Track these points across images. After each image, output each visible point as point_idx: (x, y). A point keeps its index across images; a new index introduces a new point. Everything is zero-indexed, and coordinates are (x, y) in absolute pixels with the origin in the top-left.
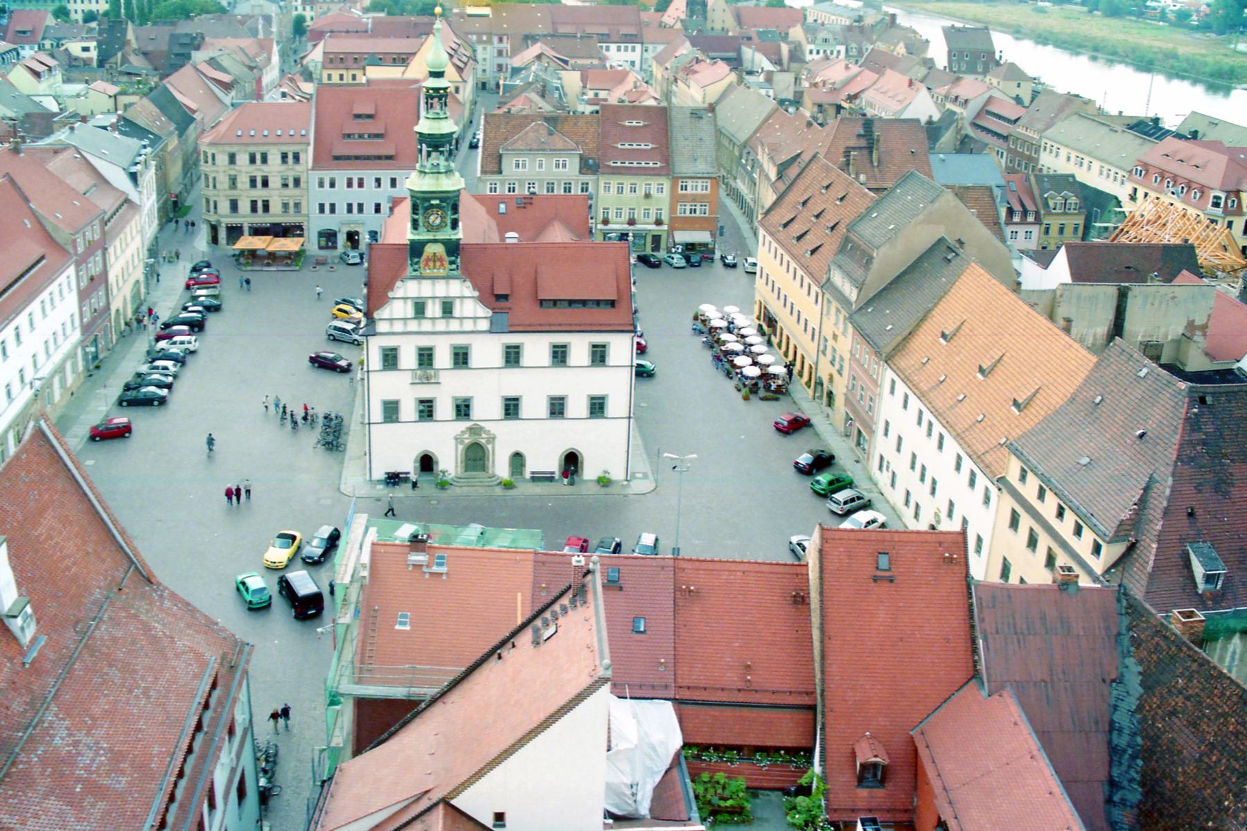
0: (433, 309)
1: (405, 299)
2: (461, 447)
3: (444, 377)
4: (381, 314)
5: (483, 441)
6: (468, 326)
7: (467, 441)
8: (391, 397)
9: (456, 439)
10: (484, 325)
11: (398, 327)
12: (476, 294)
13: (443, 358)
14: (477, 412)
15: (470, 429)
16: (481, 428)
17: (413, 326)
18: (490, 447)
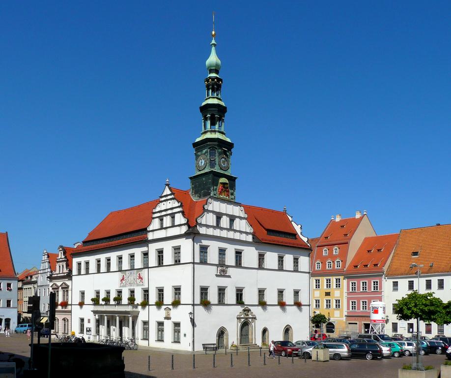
0: (225, 222)
1: (213, 212)
2: (239, 324)
3: (230, 271)
4: (203, 220)
5: (250, 320)
6: (243, 237)
7: (242, 320)
8: (205, 284)
9: (238, 318)
10: (250, 238)
11: (210, 232)
12: (246, 216)
13: (230, 259)
14: (246, 299)
15: (244, 310)
16: (249, 310)
17: (217, 233)
18: (253, 324)
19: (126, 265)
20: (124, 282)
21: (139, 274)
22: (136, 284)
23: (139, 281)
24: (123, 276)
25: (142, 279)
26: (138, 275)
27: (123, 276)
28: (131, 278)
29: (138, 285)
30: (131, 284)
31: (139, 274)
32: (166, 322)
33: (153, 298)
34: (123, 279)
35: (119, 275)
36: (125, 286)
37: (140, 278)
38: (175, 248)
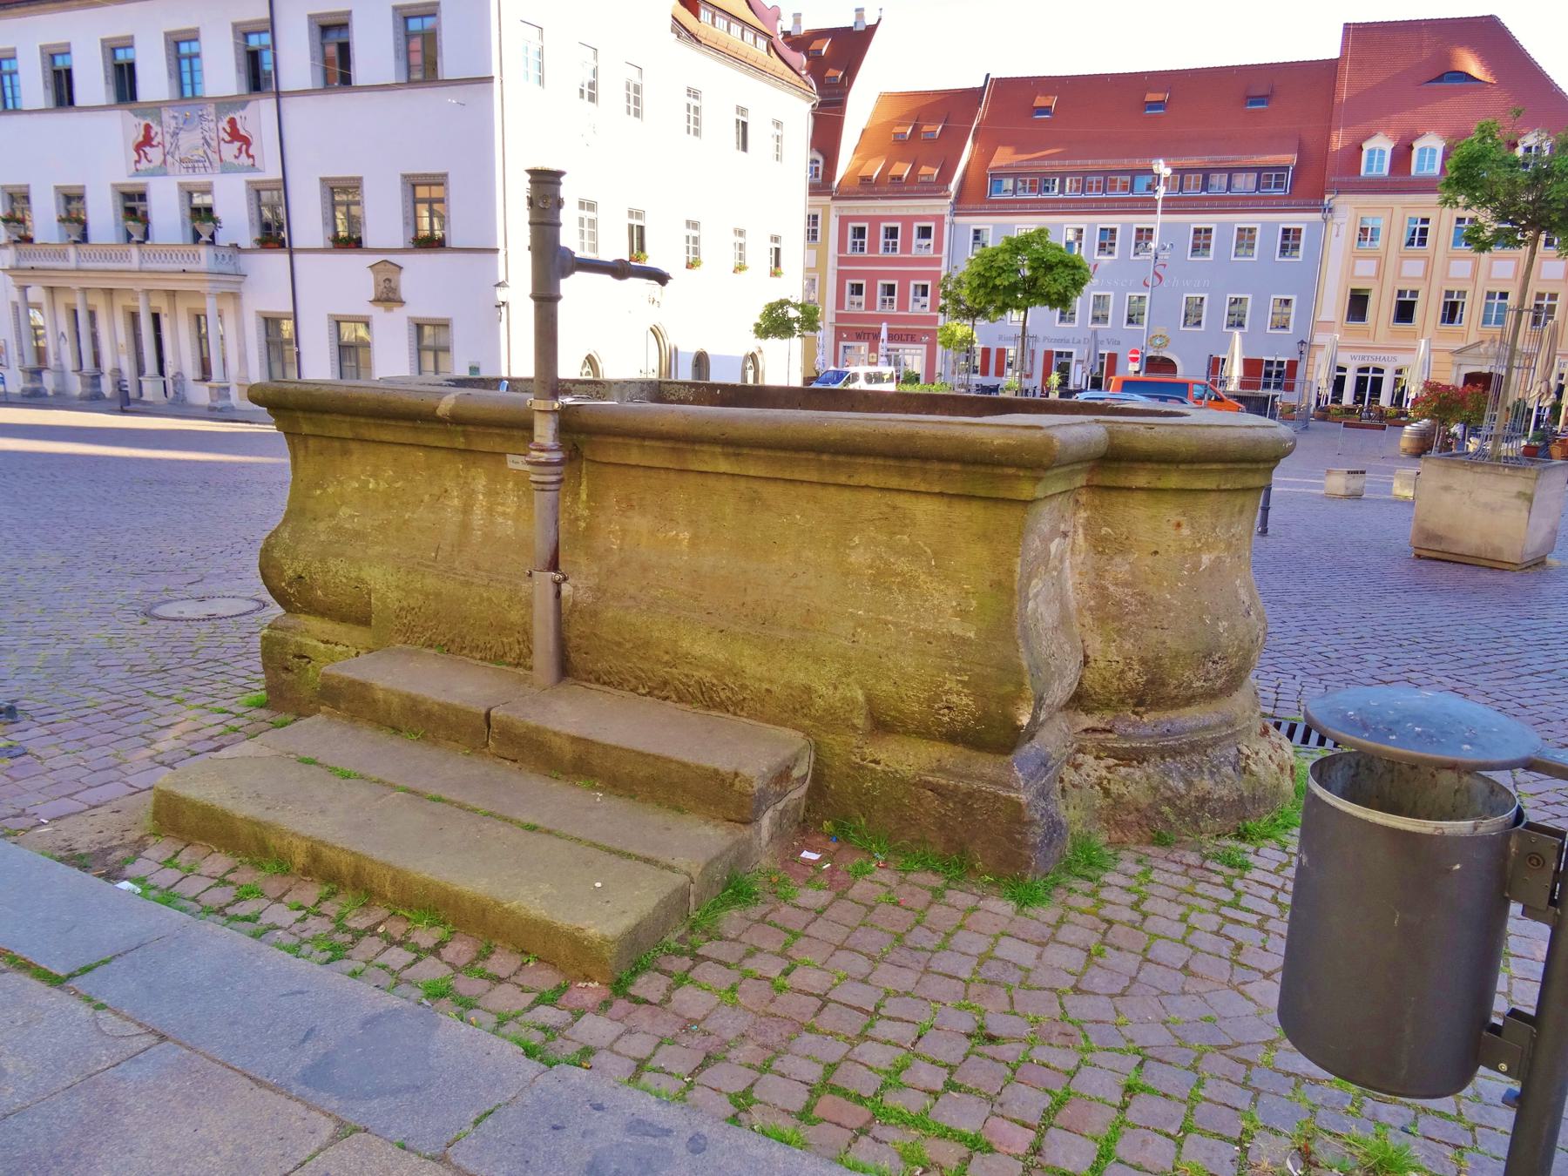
19: (153, 83)
20: (155, 154)
21: (232, 122)
22: (217, 163)
23: (229, 151)
24: (148, 128)
25: (246, 141)
26: (224, 124)
27: (148, 128)
28: (190, 141)
29: (226, 169)
30: (190, 164)
31: (232, 122)
32: (377, 314)
33: (308, 224)
34: (147, 141)
35: (121, 127)
36: (162, 170)
37: (235, 135)
38: (407, 12)
